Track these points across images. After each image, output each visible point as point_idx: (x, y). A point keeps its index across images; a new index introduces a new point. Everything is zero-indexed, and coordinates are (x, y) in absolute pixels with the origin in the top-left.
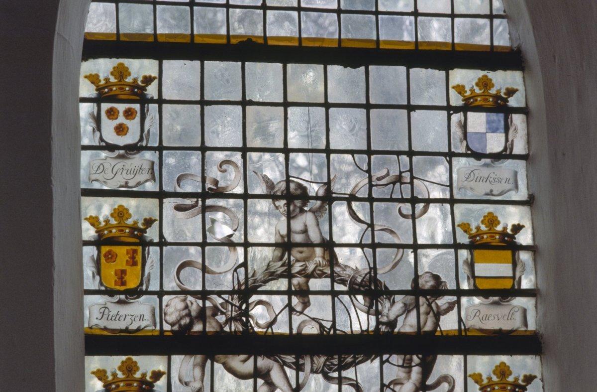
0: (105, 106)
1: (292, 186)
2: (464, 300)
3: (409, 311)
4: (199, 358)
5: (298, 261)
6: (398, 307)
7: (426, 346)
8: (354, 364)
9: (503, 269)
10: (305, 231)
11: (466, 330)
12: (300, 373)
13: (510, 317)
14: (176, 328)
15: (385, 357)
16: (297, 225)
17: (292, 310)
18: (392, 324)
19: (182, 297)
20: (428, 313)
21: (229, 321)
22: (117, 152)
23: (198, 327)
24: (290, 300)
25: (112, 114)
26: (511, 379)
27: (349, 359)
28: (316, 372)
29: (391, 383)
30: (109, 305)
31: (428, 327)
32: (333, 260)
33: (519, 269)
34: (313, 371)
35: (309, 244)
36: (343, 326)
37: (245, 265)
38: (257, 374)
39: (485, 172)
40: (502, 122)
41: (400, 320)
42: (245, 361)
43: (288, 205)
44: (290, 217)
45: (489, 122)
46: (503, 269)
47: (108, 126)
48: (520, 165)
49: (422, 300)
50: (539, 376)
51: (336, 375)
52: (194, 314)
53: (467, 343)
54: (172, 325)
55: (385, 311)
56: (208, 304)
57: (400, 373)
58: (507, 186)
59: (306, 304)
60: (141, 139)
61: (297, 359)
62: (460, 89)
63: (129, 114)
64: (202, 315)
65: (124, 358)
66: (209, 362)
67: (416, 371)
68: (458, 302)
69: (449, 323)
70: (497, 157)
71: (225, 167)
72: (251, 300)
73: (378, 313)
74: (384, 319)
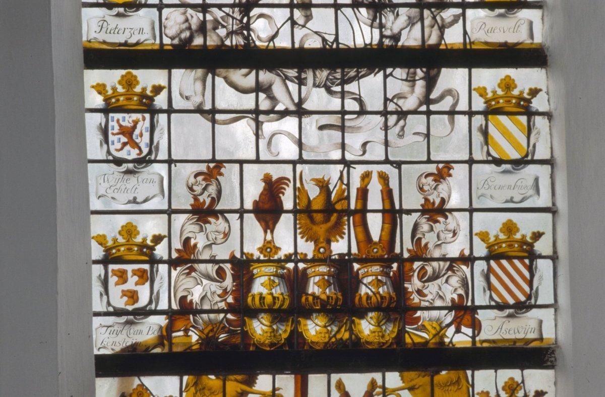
2: (470, 12)
3: (413, 24)
4: (200, 72)
6: (402, 20)
7: (430, 60)
8: (357, 78)
11: (471, 43)
12: (303, 87)
13: (516, 29)
14: (176, 41)
15: (389, 71)
17: (294, 23)
18: (396, 37)
19: (182, 10)
20: (432, 27)
21: (230, 34)
23: (198, 41)
24: (292, 13)
26: (516, 92)
27: (352, 73)
28: (319, 86)
29: (394, 97)
30: (107, 18)
31: (433, 40)
34: (315, 85)
36: (346, 40)
38: (259, 88)
41: (404, 34)
42: (246, 75)
49: (426, 13)
50: (545, 89)
51: (338, 89)
52: (194, 27)
53: (472, 57)
54: (172, 38)
55: (389, 25)
56: (209, 17)
57: (404, 87)
59: (308, 18)
61: (299, 73)
64: (202, 29)
65: (123, 72)
66: (210, 76)
67: (420, 85)
68: (464, 14)
69: (453, 37)
72: (252, 14)
73: (381, 26)
74: (387, 33)
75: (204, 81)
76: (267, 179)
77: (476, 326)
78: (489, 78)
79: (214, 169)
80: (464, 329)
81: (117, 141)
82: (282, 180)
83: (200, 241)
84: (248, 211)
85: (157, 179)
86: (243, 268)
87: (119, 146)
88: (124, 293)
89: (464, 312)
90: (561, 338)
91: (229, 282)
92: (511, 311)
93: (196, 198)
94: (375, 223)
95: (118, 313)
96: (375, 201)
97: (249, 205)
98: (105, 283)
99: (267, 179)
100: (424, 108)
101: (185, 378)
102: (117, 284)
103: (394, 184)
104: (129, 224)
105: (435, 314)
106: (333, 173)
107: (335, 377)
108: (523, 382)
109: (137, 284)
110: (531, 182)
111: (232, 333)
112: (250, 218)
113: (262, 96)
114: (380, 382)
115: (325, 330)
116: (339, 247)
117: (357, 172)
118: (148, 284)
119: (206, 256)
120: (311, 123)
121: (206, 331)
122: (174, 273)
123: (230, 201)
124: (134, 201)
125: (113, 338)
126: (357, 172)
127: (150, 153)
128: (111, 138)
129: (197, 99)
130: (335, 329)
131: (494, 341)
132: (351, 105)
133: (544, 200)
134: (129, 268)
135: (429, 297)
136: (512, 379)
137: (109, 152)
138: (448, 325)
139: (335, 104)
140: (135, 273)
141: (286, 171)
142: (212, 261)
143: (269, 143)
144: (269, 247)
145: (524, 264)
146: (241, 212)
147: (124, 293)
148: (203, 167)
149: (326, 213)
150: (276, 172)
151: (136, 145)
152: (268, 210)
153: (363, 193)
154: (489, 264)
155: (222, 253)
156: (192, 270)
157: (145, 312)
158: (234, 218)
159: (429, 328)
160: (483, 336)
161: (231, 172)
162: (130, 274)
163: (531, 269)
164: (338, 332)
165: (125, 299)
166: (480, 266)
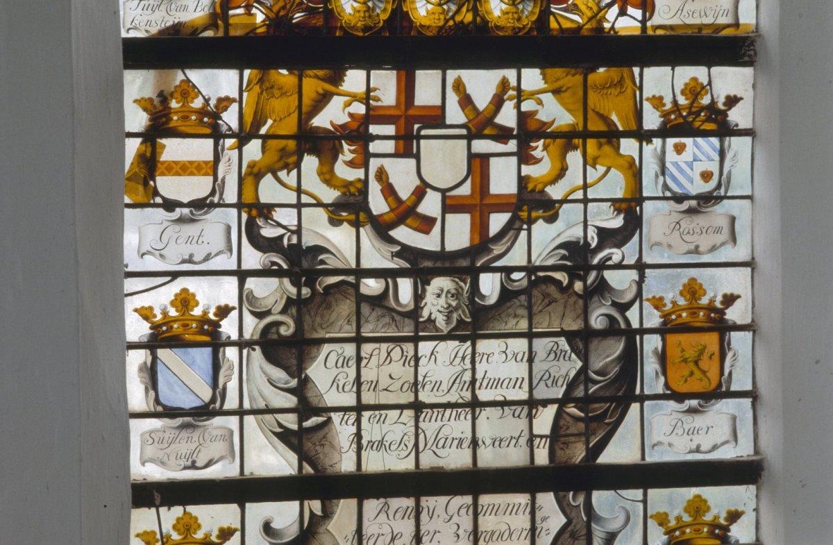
80: (630, 10)
90: (765, 25)
101: (247, 73)
107: (452, 75)
108: (710, 83)
111: (311, 12)
114: (513, 82)
115: (439, 9)
121: (275, 9)
125: (147, 15)
130: (454, 8)
131: (672, 27)
136: (695, 79)
159: (583, 8)
160: (657, 20)
164: (458, 12)
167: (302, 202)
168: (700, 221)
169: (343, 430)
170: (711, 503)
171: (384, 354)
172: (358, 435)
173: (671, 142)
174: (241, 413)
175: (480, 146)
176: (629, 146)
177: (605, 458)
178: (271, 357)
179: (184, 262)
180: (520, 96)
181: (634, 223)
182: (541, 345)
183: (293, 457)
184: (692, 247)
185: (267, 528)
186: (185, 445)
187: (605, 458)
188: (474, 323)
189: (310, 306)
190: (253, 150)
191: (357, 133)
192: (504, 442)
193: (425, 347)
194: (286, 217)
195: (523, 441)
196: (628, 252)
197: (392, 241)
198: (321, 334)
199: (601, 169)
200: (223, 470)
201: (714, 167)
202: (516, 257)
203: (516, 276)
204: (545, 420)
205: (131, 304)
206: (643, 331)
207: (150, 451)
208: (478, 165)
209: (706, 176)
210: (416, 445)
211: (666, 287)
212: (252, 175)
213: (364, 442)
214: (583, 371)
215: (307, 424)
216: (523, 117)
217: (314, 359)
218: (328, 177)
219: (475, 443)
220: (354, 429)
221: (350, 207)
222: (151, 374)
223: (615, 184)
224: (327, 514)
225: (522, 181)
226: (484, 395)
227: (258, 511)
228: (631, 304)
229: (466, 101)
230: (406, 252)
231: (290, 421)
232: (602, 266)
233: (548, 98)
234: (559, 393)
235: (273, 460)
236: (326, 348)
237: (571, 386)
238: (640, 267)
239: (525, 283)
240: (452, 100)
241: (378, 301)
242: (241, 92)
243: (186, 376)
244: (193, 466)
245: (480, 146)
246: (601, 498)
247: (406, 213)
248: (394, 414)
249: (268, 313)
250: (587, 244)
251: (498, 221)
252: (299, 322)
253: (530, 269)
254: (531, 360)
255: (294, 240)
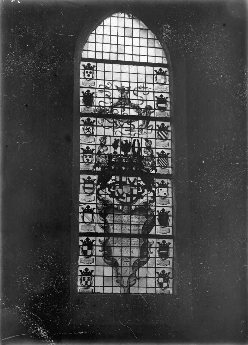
0: (86, 71)
1: (122, 88)
4: (102, 119)
5: (123, 102)
9: (164, 105)
10: (125, 96)
12: (123, 123)
16: (123, 95)
21: (109, 112)
22: (88, 80)
25: (87, 72)
27: (132, 121)
28: (126, 123)
30: (86, 108)
32: (130, 102)
33: (167, 105)
34: (125, 122)
35: (125, 99)
37: (112, 102)
39: (161, 87)
40: (164, 77)
41: (143, 114)
42: (111, 120)
43: (121, 91)
44: (121, 94)
45: (161, 77)
46: (164, 105)
47: (86, 75)
48: (168, 86)
51: (129, 123)
53: (155, 119)
56: (105, 109)
58: (165, 90)
59: (124, 110)
60: (93, 78)
62: (156, 71)
63: (90, 73)
66: (104, 120)
68: (155, 111)
69: (152, 115)
70: (163, 84)
71: (109, 84)
75: (103, 120)
76: (115, 139)
77: (156, 170)
78: (159, 123)
79: (105, 137)
81: (86, 131)
82: (118, 140)
83: (102, 150)
84: (112, 146)
85: (93, 138)
86: (110, 156)
87: (86, 132)
88: (87, 159)
89: (154, 168)
91: (107, 158)
92: (163, 168)
93: (101, 142)
94: (136, 150)
95: (85, 163)
96: (136, 145)
97: (111, 144)
98: (83, 157)
99: (115, 139)
100: (146, 128)
102: (85, 157)
103: (140, 142)
104: (88, 146)
105: (148, 167)
106: (128, 139)
107: (127, 177)
109: (89, 158)
110: (167, 143)
112: (112, 147)
113: (114, 124)
116: (129, 153)
117: (133, 139)
118: (91, 158)
119: (103, 153)
120: (124, 129)
122: (97, 156)
123: (108, 143)
124: (89, 142)
126: (133, 139)
127: (92, 133)
128: (85, 130)
129: (102, 124)
132: (132, 127)
133: (170, 147)
134: (88, 155)
135: (147, 164)
137: (84, 133)
138: (150, 170)
139: (129, 126)
140: (89, 156)
141: (119, 138)
142: (104, 154)
143: (116, 133)
144: (115, 153)
145: (165, 159)
146: (110, 146)
147: (87, 159)
148: (103, 137)
149: (126, 147)
150: (117, 138)
151: (89, 132)
152: (115, 145)
153: (134, 143)
154: (159, 158)
155: (106, 153)
156: (100, 156)
157: (91, 163)
158: (109, 147)
161: (108, 138)
162: (88, 156)
163: (167, 160)
165: (87, 160)
166: (157, 159)
167: (106, 194)
168: (164, 200)
169: (111, 227)
170: (166, 241)
171: (117, 216)
172: (113, 228)
173: (160, 189)
174: (96, 223)
175: (132, 187)
176: (153, 189)
177: (150, 233)
178: (100, 215)
179: (88, 201)
180: (138, 181)
181: (154, 200)
182: (141, 217)
183: (103, 231)
184: (163, 204)
185: (100, 240)
186: (88, 228)
187: (150, 233)
188: (131, 213)
189: (106, 209)
190: (99, 186)
191: (113, 185)
192: (135, 230)
193: (123, 216)
194: (103, 196)
195: (138, 230)
196: (154, 204)
197: (119, 200)
198: (108, 213)
199: (150, 192)
200: (93, 231)
201: (166, 193)
202: (137, 203)
203: (137, 206)
204: (141, 227)
205: (80, 207)
206: (156, 216)
207: (83, 228)
208: (132, 190)
209: (165, 194)
210: (122, 230)
211: (159, 209)
212: (98, 191)
213: (114, 229)
214: (147, 221)
215: (106, 226)
216: (138, 184)
217: (107, 216)
218: (109, 190)
219: (130, 230)
220: (112, 227)
221: (112, 195)
222: (83, 217)
223: (151, 194)
224: (109, 239)
225: (138, 193)
226: (132, 223)
227: (98, 238)
228: (154, 212)
229: (130, 181)
230: (121, 202)
231: (103, 225)
232: (150, 206)
233: (142, 181)
234: (143, 223)
235: (100, 230)
236: (109, 215)
237: (145, 223)
238: (155, 206)
239: (138, 207)
240: (128, 181)
241: (116, 208)
242: (97, 178)
243: (88, 217)
244: (89, 231)
245: (132, 187)
246: (150, 240)
247: (121, 196)
248: (118, 225)
249: (100, 209)
250: (148, 202)
251: (134, 198)
252: (105, 211)
253: (139, 205)
254: (139, 219)
255: (104, 199)
